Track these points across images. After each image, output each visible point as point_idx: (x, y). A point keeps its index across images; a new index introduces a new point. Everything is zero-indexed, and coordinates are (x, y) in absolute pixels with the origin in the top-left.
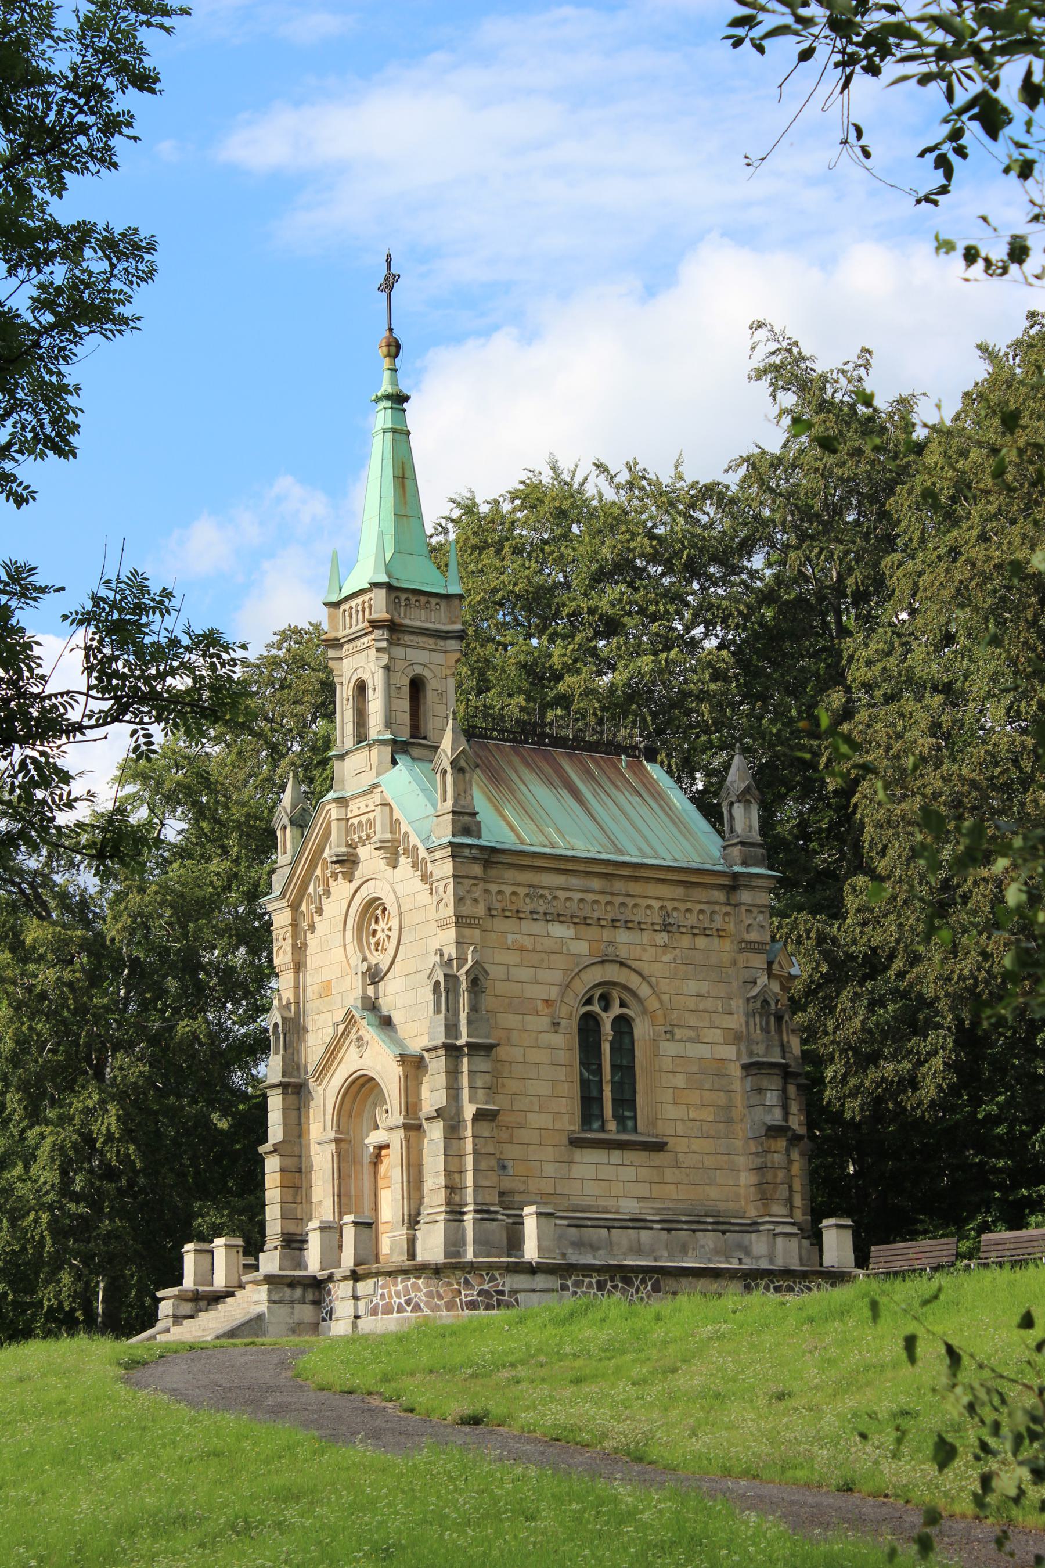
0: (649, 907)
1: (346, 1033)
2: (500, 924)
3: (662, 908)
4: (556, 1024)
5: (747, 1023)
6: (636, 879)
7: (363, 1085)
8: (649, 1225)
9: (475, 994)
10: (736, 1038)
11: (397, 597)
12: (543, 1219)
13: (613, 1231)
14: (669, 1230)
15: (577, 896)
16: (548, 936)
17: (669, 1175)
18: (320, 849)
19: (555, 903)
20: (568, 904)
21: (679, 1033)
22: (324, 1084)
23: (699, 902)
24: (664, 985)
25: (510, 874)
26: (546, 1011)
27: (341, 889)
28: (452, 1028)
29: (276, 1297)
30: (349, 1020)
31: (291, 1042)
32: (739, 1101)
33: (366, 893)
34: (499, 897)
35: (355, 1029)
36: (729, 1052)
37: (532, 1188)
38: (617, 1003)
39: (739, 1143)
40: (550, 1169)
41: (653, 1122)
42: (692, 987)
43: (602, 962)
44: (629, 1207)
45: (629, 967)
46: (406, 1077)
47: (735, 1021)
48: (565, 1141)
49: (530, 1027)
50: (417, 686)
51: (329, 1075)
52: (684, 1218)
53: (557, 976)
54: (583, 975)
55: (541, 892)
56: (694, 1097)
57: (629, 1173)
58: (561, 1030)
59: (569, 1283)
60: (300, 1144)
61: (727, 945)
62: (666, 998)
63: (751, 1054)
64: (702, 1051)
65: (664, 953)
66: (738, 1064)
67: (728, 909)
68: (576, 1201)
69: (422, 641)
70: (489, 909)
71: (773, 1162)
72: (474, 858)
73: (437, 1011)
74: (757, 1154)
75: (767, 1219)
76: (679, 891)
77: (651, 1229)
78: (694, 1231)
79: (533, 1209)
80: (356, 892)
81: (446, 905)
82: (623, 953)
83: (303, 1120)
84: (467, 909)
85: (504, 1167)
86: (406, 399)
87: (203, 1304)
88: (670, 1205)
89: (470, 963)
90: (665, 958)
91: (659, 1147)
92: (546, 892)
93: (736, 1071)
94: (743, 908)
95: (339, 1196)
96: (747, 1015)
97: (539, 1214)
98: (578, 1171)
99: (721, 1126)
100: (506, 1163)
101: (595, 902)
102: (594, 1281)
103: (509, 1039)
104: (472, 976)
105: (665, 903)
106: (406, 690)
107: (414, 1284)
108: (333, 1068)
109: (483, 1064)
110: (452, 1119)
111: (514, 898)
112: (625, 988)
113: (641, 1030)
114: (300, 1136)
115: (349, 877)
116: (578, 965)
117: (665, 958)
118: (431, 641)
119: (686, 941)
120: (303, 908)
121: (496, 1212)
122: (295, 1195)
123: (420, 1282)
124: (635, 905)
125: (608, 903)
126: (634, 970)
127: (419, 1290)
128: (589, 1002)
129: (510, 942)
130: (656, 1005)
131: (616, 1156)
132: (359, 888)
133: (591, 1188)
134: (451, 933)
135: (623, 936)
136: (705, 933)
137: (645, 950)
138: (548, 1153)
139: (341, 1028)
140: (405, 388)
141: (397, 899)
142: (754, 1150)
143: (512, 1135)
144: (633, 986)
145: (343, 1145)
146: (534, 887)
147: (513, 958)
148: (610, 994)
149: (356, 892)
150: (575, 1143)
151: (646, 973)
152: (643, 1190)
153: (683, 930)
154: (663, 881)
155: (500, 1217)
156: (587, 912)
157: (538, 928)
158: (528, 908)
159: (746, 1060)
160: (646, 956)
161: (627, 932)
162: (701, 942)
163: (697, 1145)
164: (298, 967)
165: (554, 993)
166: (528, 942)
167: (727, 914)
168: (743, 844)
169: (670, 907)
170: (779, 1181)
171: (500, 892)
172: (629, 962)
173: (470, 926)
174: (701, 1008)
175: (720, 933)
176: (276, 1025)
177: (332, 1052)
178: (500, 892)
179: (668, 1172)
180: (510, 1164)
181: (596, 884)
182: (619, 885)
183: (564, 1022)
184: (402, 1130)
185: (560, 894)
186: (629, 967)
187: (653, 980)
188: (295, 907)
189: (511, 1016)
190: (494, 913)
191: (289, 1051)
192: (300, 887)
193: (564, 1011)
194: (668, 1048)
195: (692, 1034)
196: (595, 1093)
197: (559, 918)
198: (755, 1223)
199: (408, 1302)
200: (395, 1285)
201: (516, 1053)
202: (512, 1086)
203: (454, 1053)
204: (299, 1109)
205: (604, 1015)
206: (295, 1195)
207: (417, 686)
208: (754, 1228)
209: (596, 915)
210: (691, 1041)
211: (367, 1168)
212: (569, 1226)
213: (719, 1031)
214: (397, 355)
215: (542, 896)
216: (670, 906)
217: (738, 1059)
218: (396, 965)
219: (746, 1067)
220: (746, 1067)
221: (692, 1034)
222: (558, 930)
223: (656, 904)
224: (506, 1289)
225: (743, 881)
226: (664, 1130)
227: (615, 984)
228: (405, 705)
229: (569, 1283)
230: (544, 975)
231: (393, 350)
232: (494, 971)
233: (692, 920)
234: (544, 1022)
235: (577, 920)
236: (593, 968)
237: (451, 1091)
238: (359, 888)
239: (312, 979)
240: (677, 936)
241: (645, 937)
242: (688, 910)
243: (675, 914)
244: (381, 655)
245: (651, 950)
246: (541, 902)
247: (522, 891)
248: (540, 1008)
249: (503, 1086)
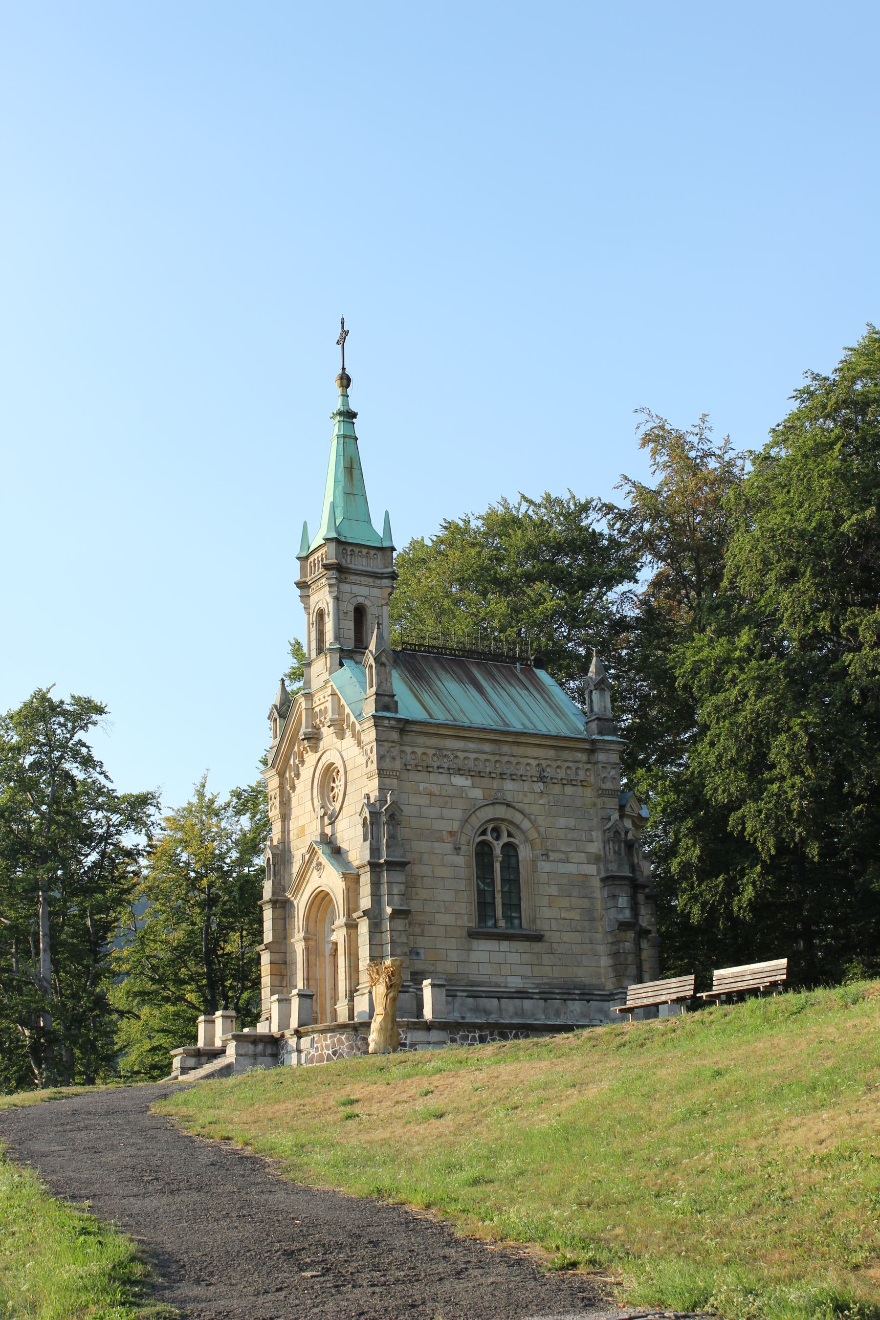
0: (528, 764)
1: (310, 861)
2: (414, 776)
3: (538, 765)
4: (457, 849)
5: (604, 848)
6: (518, 744)
8: (530, 995)
9: (393, 826)
10: (597, 859)
11: (344, 549)
12: (437, 989)
13: (503, 1000)
14: (546, 1000)
15: (473, 756)
16: (451, 785)
17: (546, 959)
19: (456, 761)
20: (466, 762)
21: (552, 856)
23: (566, 761)
24: (540, 821)
25: (421, 740)
26: (450, 839)
27: (311, 758)
28: (375, 851)
29: (242, 1052)
30: (312, 851)
31: (279, 871)
32: (599, 905)
34: (413, 757)
35: (316, 858)
36: (592, 869)
37: (439, 970)
38: (506, 834)
39: (599, 936)
40: (453, 955)
41: (533, 920)
42: (562, 822)
43: (493, 804)
44: (515, 983)
45: (514, 808)
46: (348, 890)
47: (595, 847)
48: (465, 934)
49: (437, 851)
50: (360, 612)
52: (557, 991)
53: (458, 814)
54: (478, 813)
55: (445, 753)
56: (565, 902)
57: (515, 958)
58: (462, 853)
59: (458, 1037)
60: (286, 944)
61: (589, 792)
62: (542, 830)
63: (607, 870)
64: (571, 868)
65: (541, 798)
66: (598, 878)
67: (589, 766)
68: (472, 977)
69: (364, 579)
70: (405, 765)
71: (624, 949)
72: (392, 727)
73: (365, 840)
74: (612, 943)
75: (620, 990)
76: (551, 753)
77: (532, 998)
78: (565, 1000)
79: (429, 981)
80: (319, 760)
81: (372, 762)
82: (509, 798)
83: (287, 926)
84: (387, 764)
85: (418, 954)
86: (354, 415)
87: (204, 1059)
88: (547, 981)
89: (389, 803)
90: (541, 802)
91: (538, 938)
92: (449, 753)
93: (596, 883)
94: (600, 765)
95: (308, 979)
96: (604, 842)
97: (433, 985)
98: (475, 956)
99: (586, 923)
100: (419, 950)
101: (487, 760)
102: (477, 1035)
103: (421, 859)
104: (390, 813)
105: (541, 762)
106: (351, 615)
107: (339, 1040)
109: (399, 877)
110: (375, 918)
111: (424, 757)
112: (511, 823)
113: (524, 853)
114: (285, 938)
115: (315, 749)
116: (474, 805)
117: (541, 802)
118: (371, 580)
119: (557, 789)
121: (409, 986)
122: (282, 981)
123: (343, 1037)
124: (518, 763)
125: (497, 761)
126: (518, 810)
127: (343, 1044)
128: (484, 833)
129: (421, 788)
130: (535, 835)
131: (505, 945)
132: (321, 757)
133: (485, 970)
134: (375, 782)
135: (509, 785)
136: (571, 783)
137: (526, 796)
138: (453, 944)
139: (307, 857)
140: (353, 408)
141: (344, 762)
142: (610, 940)
143: (423, 931)
144: (517, 822)
145: (312, 943)
146: (439, 749)
147: (424, 800)
148: (499, 827)
149: (319, 760)
150: (473, 935)
151: (527, 811)
152: (527, 970)
153: (555, 781)
154: (539, 745)
155: (411, 990)
156: (481, 767)
157: (443, 779)
158: (436, 765)
159: (603, 875)
160: (526, 800)
161: (512, 782)
162: (569, 790)
163: (567, 937)
164: (285, 817)
165: (456, 826)
166: (435, 789)
167: (588, 770)
168: (598, 719)
169: (544, 765)
170: (629, 962)
171: (413, 753)
172: (514, 804)
173: (389, 777)
174: (570, 837)
175: (583, 784)
177: (303, 875)
178: (413, 753)
179: (545, 957)
180: (422, 951)
181: (487, 747)
182: (505, 749)
183: (463, 848)
184: (345, 928)
185: (459, 754)
186: (514, 808)
187: (533, 817)
188: (281, 775)
189: (422, 843)
190: (409, 767)
191: (278, 877)
192: (284, 760)
193: (464, 840)
194: (545, 866)
195: (562, 856)
196: (489, 900)
197: (459, 771)
198: (612, 994)
199: (334, 1053)
200: (326, 1040)
201: (426, 870)
202: (424, 894)
203: (378, 870)
204: (285, 919)
205: (495, 843)
206: (282, 981)
207: (360, 612)
208: (612, 997)
209: (488, 770)
210: (561, 861)
211: (328, 959)
212: (467, 997)
213: (583, 854)
214: (348, 386)
215: (446, 756)
216: (544, 763)
217: (598, 875)
218: (344, 809)
219: (603, 880)
220: (603, 880)
221: (562, 856)
222: (459, 781)
223: (534, 762)
224: (407, 1042)
225: (599, 745)
226: (541, 926)
227: (503, 820)
228: (351, 625)
229: (458, 1037)
230: (446, 813)
231: (345, 382)
232: (407, 810)
233: (562, 774)
234: (448, 847)
235: (473, 774)
236: (486, 808)
237: (374, 898)
238: (321, 757)
239: (293, 825)
240: (551, 786)
241: (526, 786)
242: (558, 767)
243: (548, 770)
244: (333, 589)
246: (445, 760)
247: (431, 752)
248: (445, 837)
249: (417, 894)
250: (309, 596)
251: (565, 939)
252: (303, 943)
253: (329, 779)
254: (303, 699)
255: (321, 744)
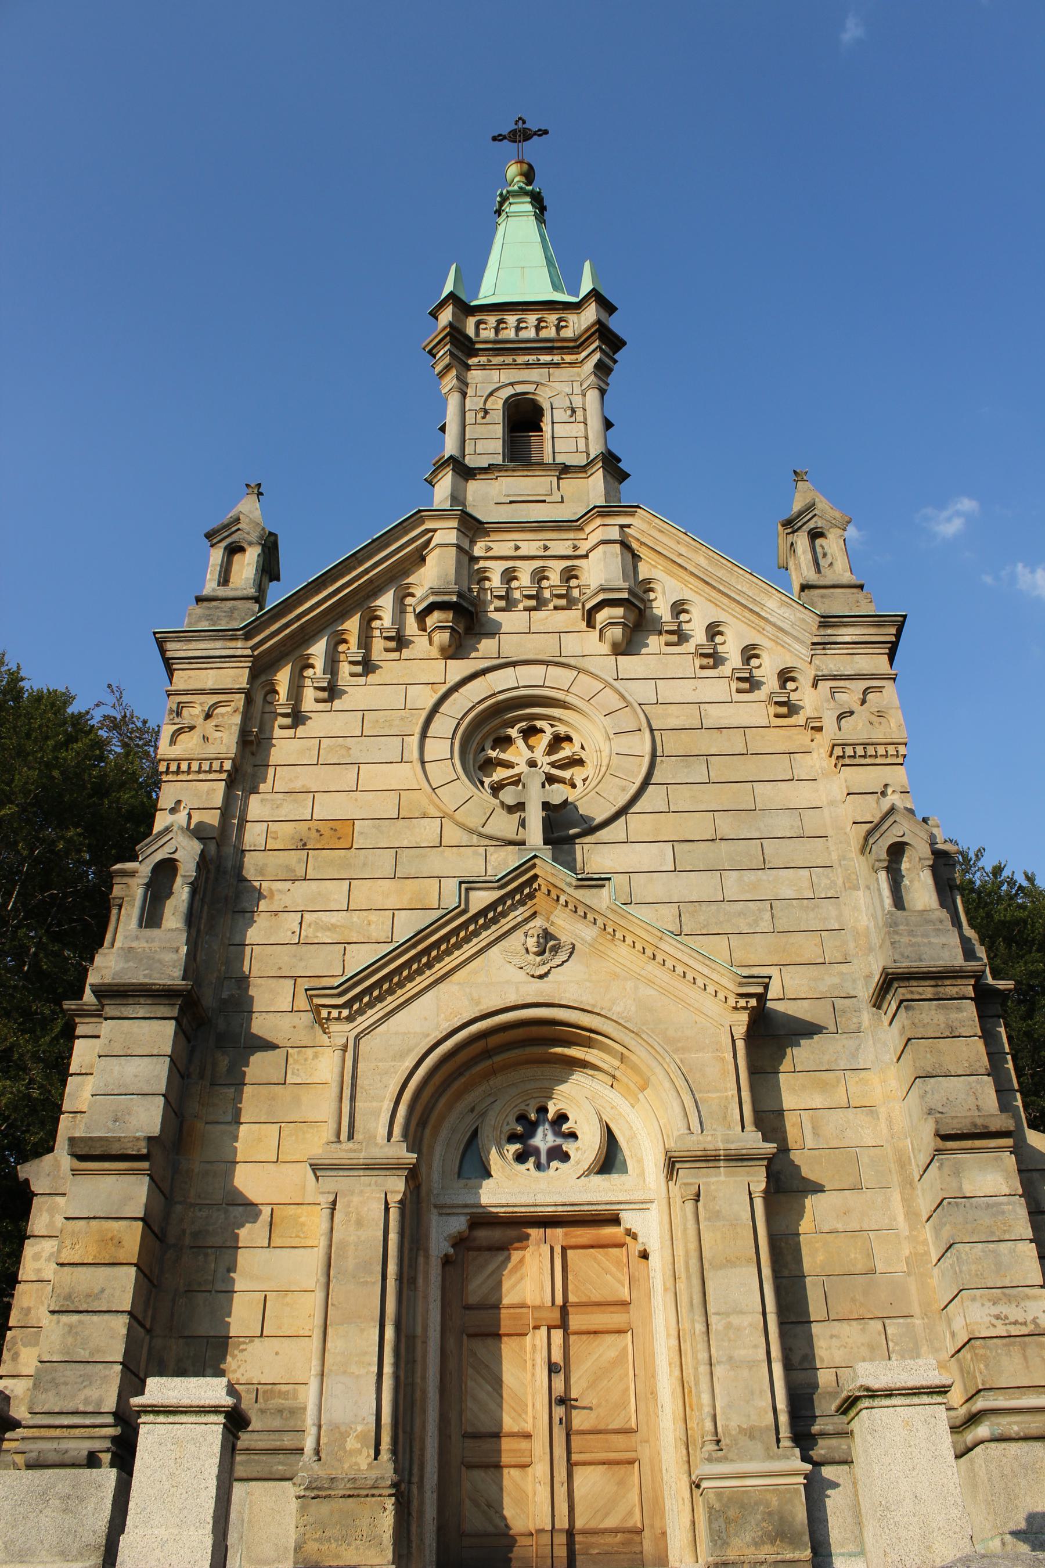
1: (490, 914)
7: (487, 1054)
18: (375, 589)
22: (364, 1021)
33: (503, 681)
51: (391, 1003)
108: (411, 988)
115: (456, 650)
120: (283, 678)
139: (480, 899)
176: (166, 869)
250: (468, 368)
252: (397, 1186)
253: (485, 738)
254: (454, 524)
255: (487, 646)
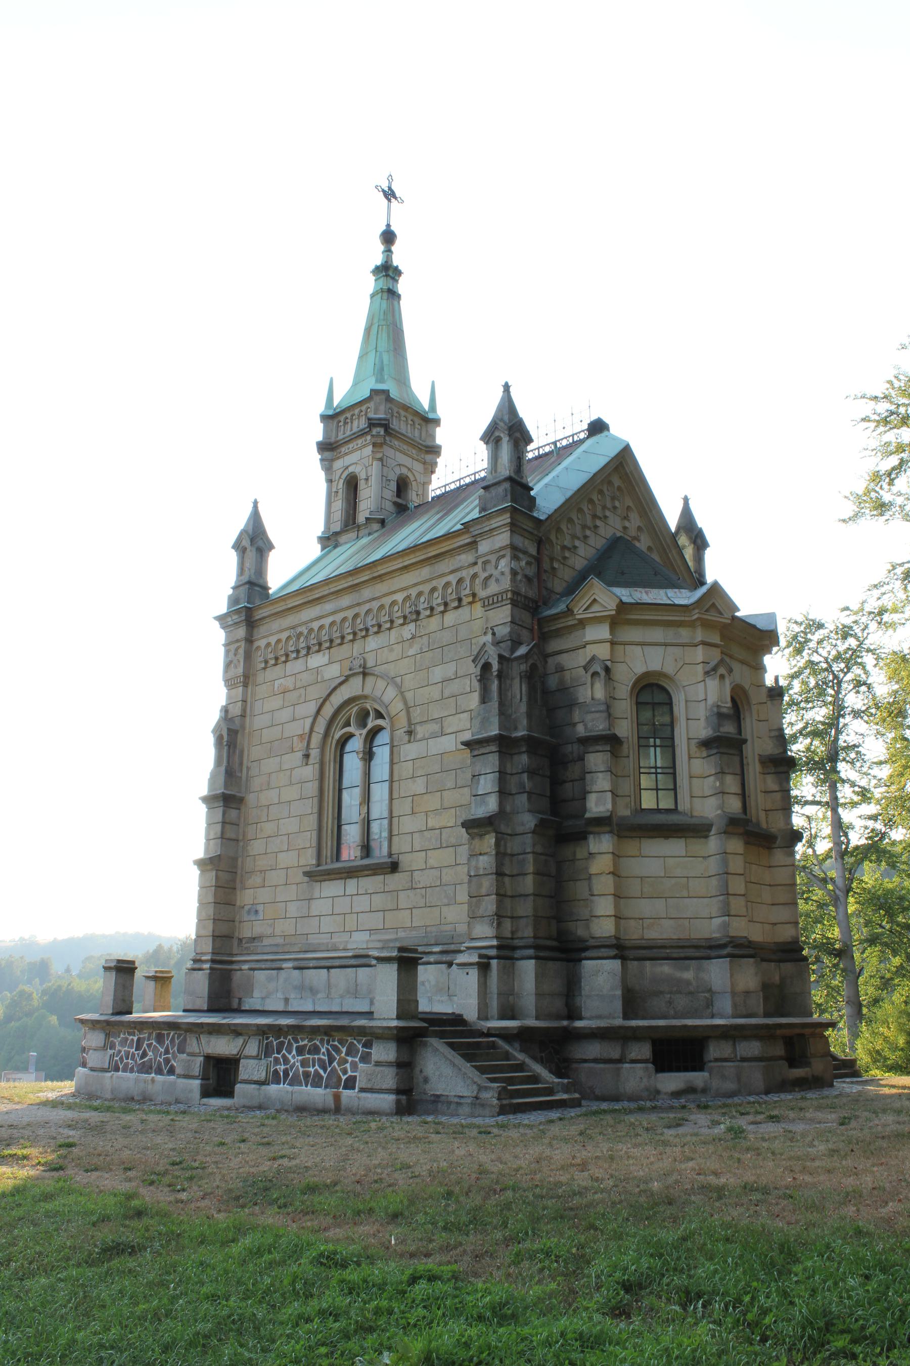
6: (380, 578)
13: (332, 971)
17: (405, 899)
21: (420, 731)
24: (409, 682)
25: (276, 625)
40: (293, 909)
44: (359, 941)
56: (433, 802)
57: (362, 903)
59: (117, 1041)
65: (411, 646)
68: (313, 940)
71: (477, 868)
91: (394, 867)
98: (320, 907)
102: (135, 1038)
131: (352, 885)
133: (328, 925)
150: (316, 875)
152: (376, 920)
154: (406, 568)
163: (436, 858)
170: (484, 891)
174: (446, 694)
180: (260, 908)
181: (346, 601)
182: (367, 593)
195: (435, 727)
207: (352, 484)
210: (434, 736)
213: (465, 715)
221: (435, 727)
245: (398, 648)
251: (432, 862)
